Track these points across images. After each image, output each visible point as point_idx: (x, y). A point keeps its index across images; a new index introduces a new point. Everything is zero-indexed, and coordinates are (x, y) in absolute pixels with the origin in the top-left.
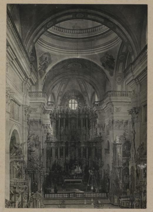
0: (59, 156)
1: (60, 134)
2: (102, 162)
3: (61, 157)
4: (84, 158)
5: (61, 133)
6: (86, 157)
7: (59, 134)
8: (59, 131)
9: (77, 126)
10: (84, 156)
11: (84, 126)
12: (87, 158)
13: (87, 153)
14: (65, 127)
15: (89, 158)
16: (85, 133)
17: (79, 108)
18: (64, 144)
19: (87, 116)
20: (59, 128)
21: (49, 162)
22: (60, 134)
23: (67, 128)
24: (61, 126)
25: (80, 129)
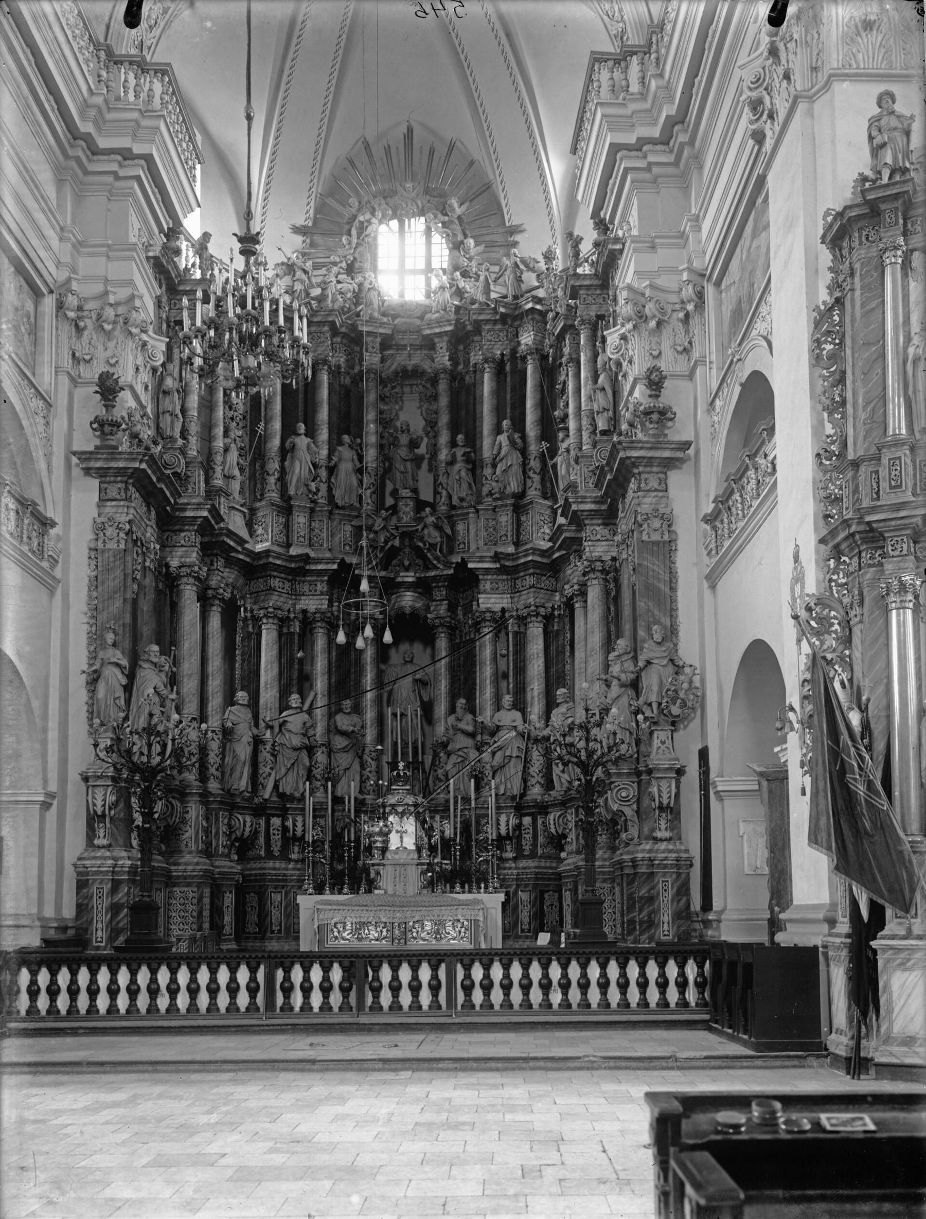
0: (268, 695)
1: (286, 497)
2: (679, 669)
3: (284, 706)
4: (509, 717)
5: (292, 492)
6: (520, 705)
7: (274, 495)
8: (274, 465)
9: (444, 438)
10: (507, 699)
11: (506, 423)
12: (536, 709)
13: (536, 667)
14: (334, 443)
15: (550, 704)
16: (514, 486)
17: (462, 284)
18: (321, 587)
19: (527, 338)
20: (276, 442)
21: (114, 678)
22: (286, 497)
23: (346, 453)
24: (288, 430)
25: (468, 460)
